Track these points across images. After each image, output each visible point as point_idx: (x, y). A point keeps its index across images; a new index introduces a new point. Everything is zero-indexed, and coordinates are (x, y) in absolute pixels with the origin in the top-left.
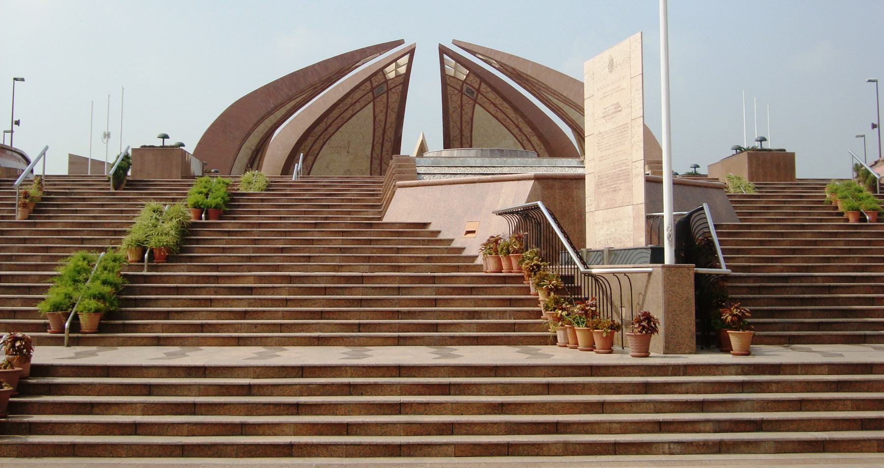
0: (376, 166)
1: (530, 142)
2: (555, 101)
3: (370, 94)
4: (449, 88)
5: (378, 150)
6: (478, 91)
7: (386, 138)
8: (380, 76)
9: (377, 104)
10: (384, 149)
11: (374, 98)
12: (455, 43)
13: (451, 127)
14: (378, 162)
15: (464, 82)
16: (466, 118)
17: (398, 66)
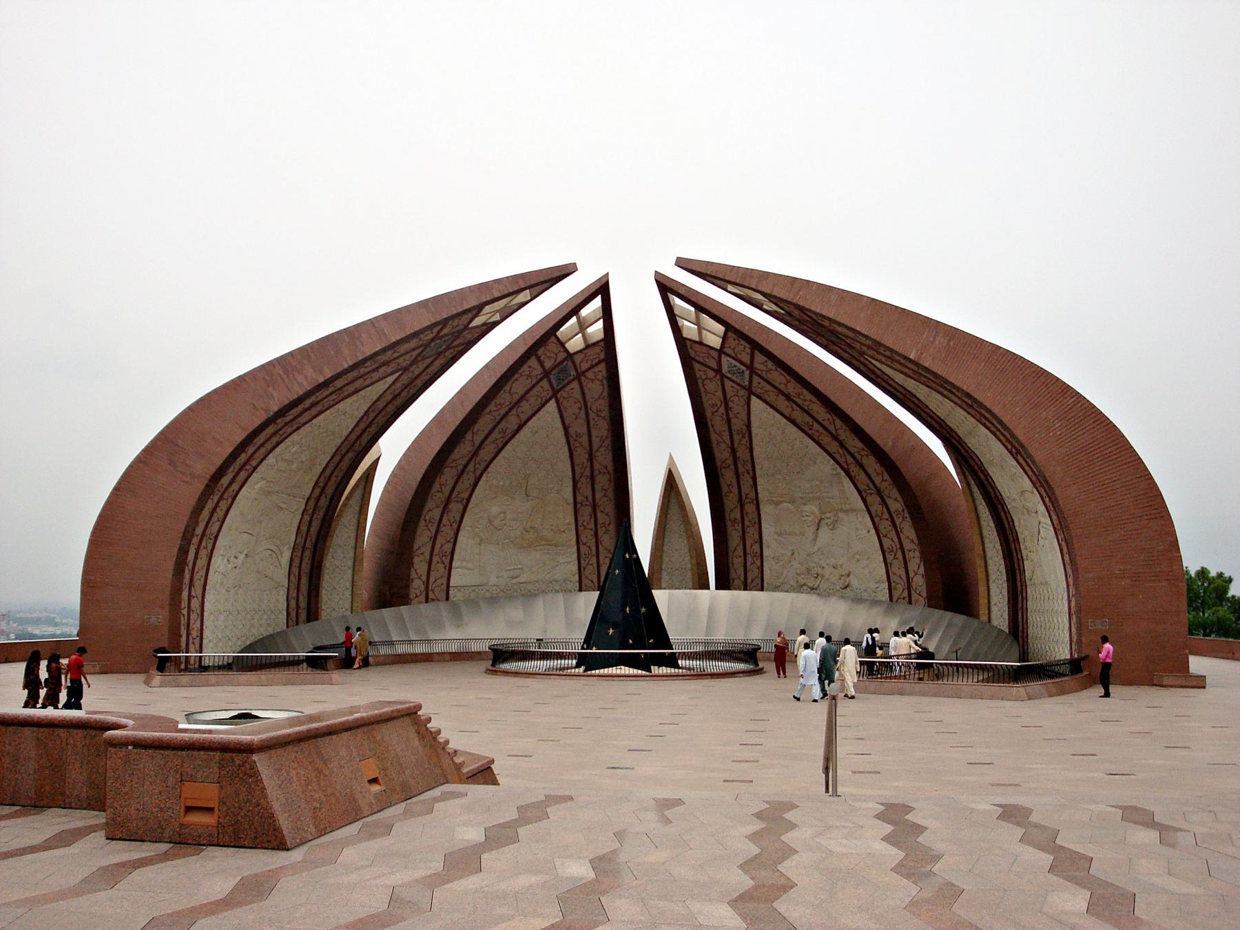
0: (586, 518)
1: (862, 467)
2: (899, 378)
3: (545, 383)
4: (697, 366)
5: (585, 490)
6: (751, 368)
7: (596, 466)
8: (552, 345)
9: (565, 404)
10: (598, 487)
11: (555, 394)
12: (682, 263)
13: (714, 443)
14: (590, 509)
15: (721, 351)
16: (738, 424)
17: (583, 326)
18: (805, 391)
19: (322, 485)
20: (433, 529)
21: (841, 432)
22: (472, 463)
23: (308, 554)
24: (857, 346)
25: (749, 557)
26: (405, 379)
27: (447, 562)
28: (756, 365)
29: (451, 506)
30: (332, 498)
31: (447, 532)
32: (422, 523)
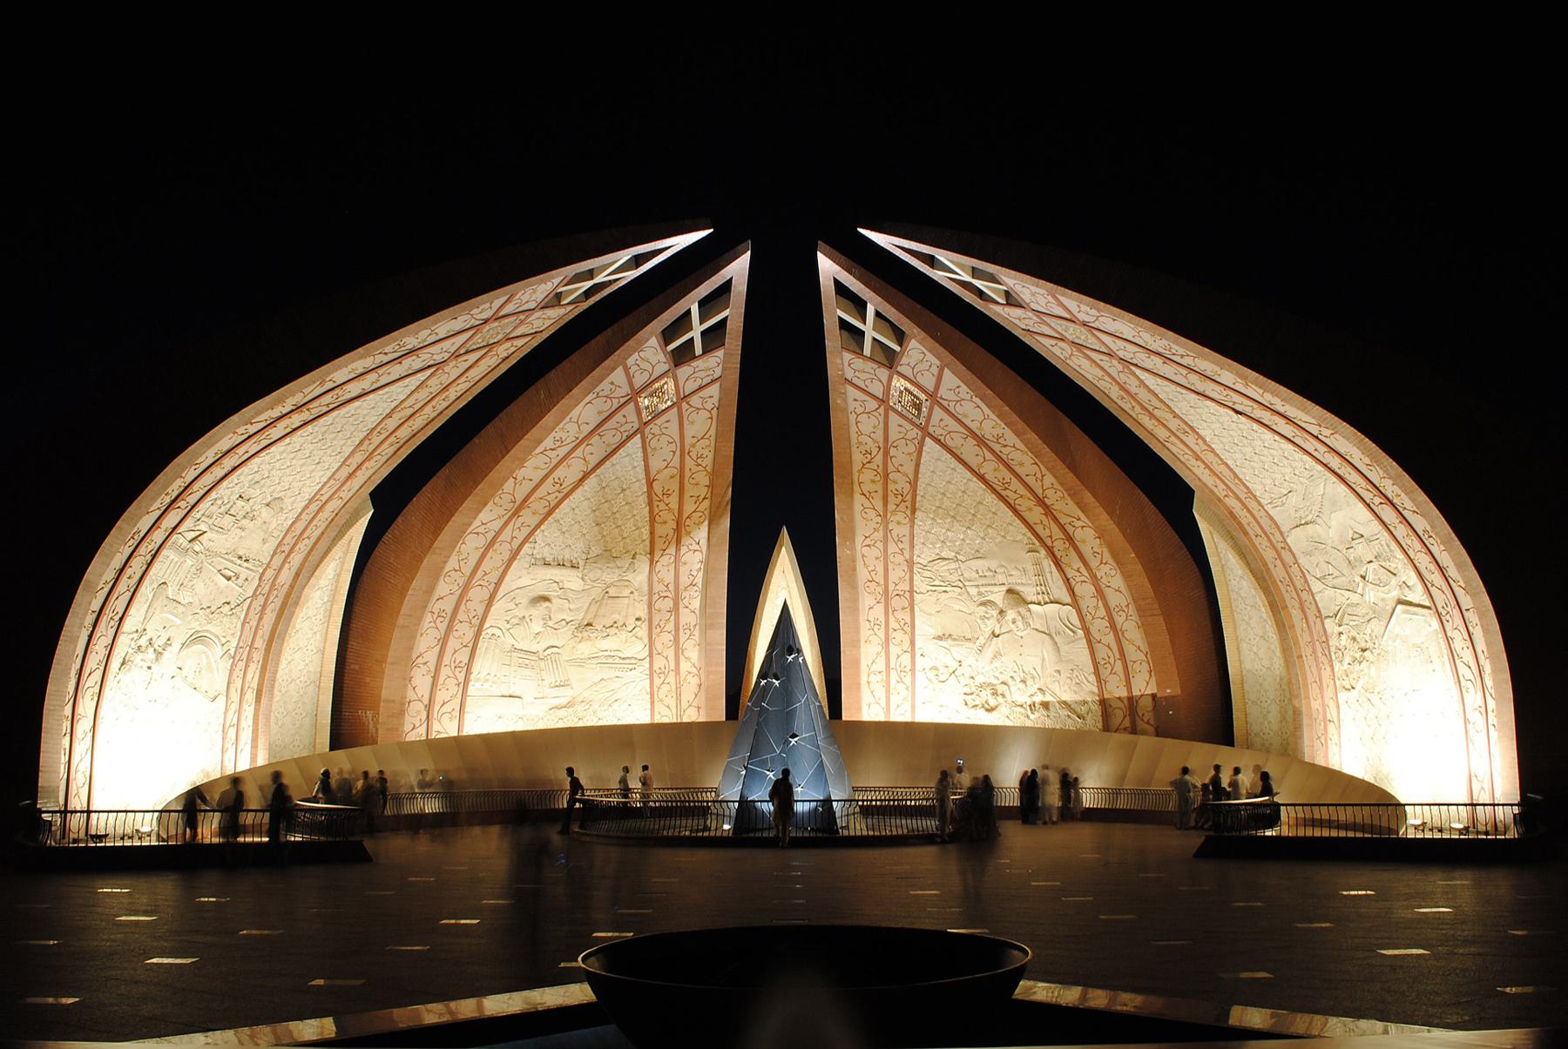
6: (933, 396)
7: (686, 541)
13: (858, 508)
18: (1008, 433)
19: (287, 549)
20: (443, 627)
21: (1050, 493)
22: (510, 527)
23: (258, 656)
24: (1128, 352)
25: (893, 673)
26: (435, 385)
27: (461, 678)
28: (943, 392)
29: (472, 593)
30: (297, 575)
31: (464, 631)
32: (428, 617)
